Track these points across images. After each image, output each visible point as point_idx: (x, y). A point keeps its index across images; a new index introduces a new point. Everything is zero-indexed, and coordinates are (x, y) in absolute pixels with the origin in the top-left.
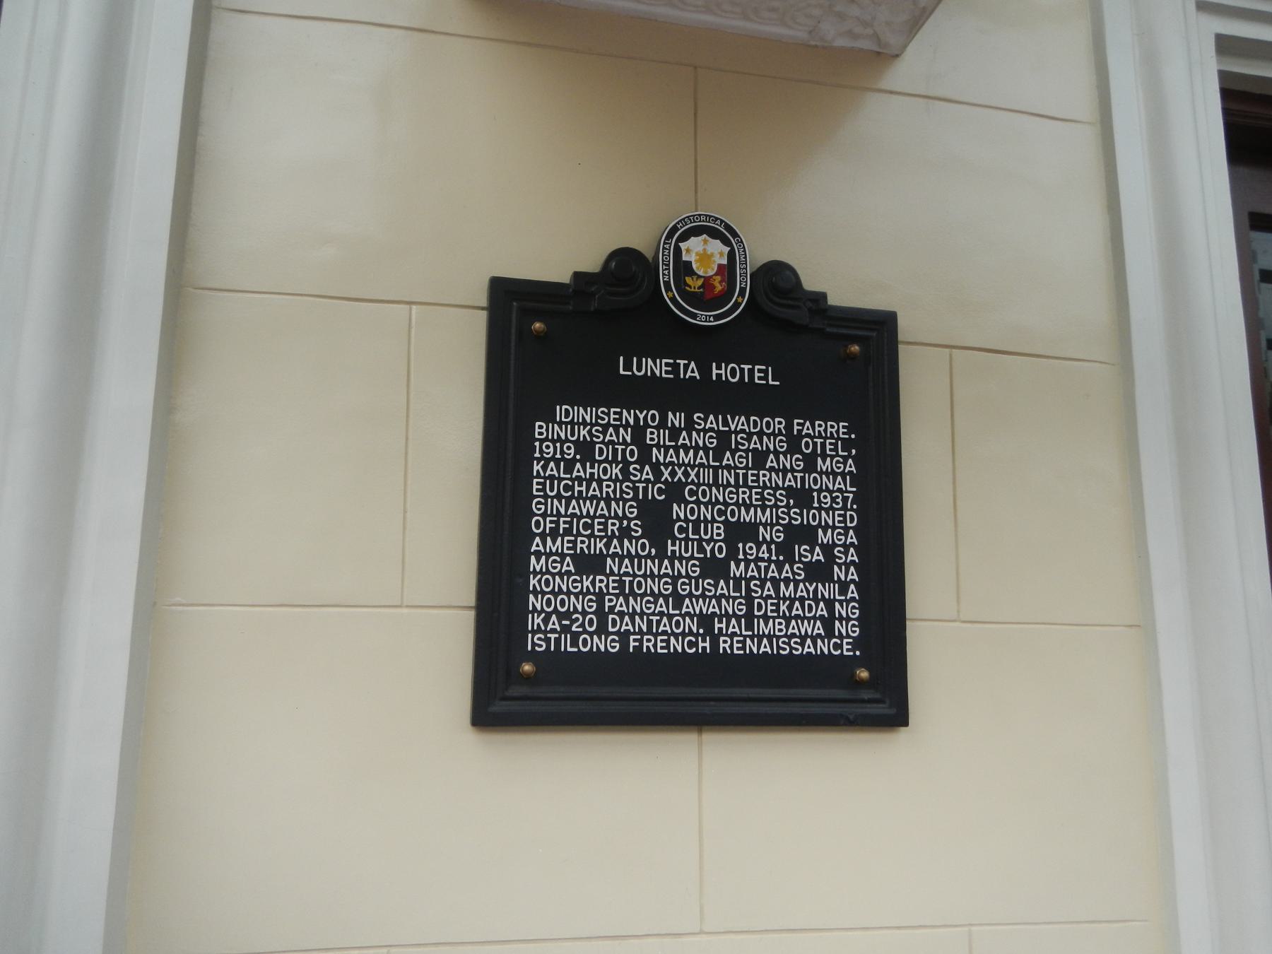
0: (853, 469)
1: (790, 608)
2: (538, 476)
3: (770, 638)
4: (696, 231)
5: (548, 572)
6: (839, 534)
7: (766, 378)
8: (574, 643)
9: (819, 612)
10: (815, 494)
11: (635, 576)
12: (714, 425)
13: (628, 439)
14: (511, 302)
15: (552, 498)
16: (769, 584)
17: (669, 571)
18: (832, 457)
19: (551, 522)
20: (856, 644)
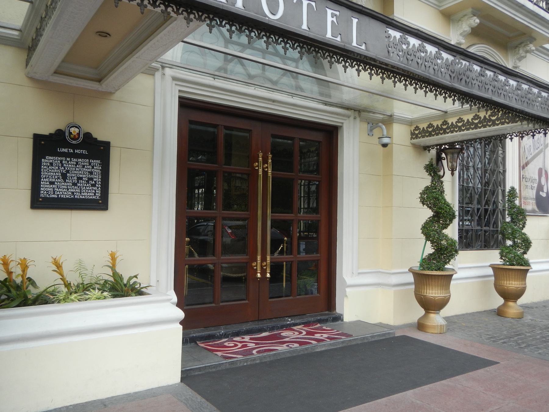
4: (73, 127)
14: (37, 138)
20: (100, 197)
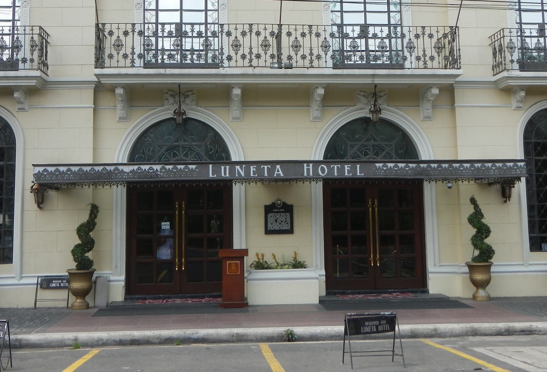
14: (266, 207)
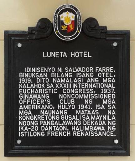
0: (114, 81)
1: (94, 123)
2: (21, 88)
3: (88, 131)
4: (65, 11)
5: (24, 115)
6: (110, 101)
7: (87, 55)
8: (32, 134)
9: (103, 124)
10: (102, 89)
11: (49, 115)
12: (71, 71)
13: (46, 76)
14: (11, 38)
15: (25, 94)
16: (88, 116)
17: (59, 113)
18: (108, 78)
19: (25, 101)
20: (114, 133)
